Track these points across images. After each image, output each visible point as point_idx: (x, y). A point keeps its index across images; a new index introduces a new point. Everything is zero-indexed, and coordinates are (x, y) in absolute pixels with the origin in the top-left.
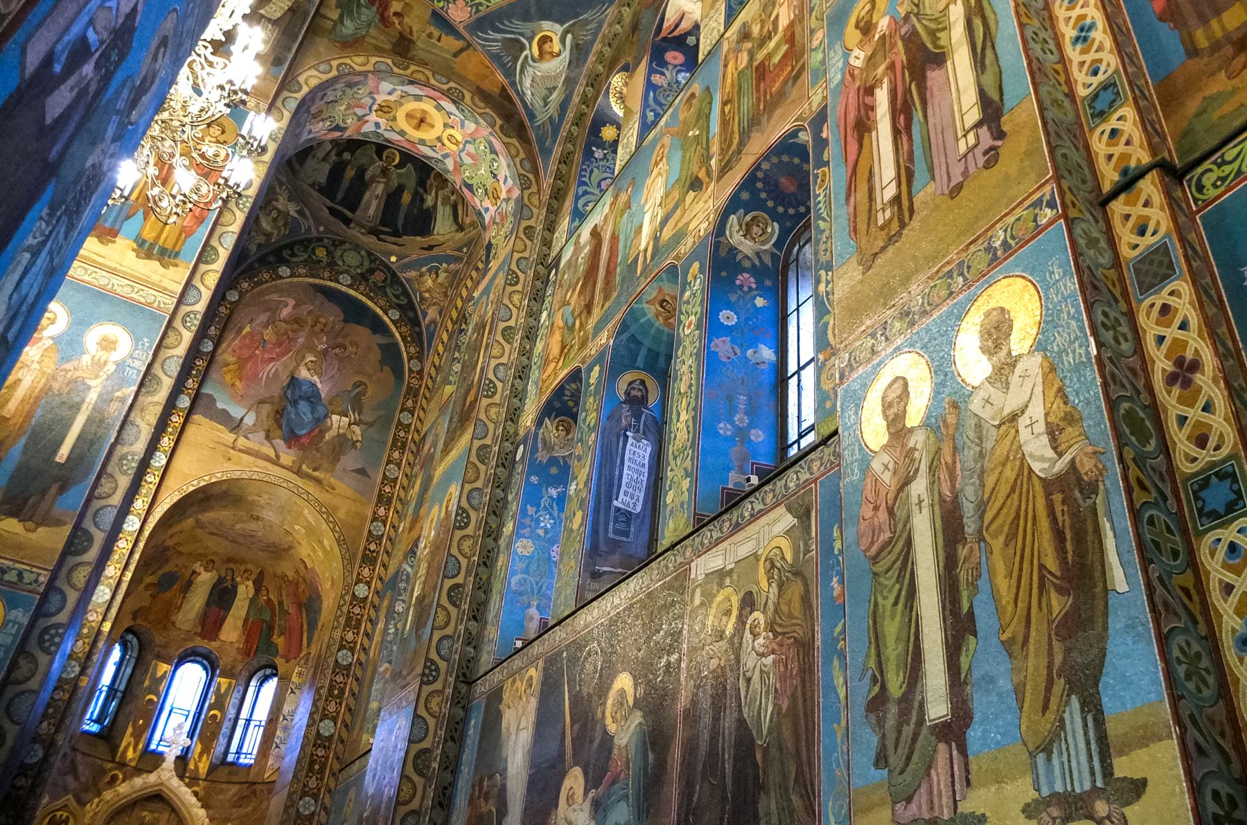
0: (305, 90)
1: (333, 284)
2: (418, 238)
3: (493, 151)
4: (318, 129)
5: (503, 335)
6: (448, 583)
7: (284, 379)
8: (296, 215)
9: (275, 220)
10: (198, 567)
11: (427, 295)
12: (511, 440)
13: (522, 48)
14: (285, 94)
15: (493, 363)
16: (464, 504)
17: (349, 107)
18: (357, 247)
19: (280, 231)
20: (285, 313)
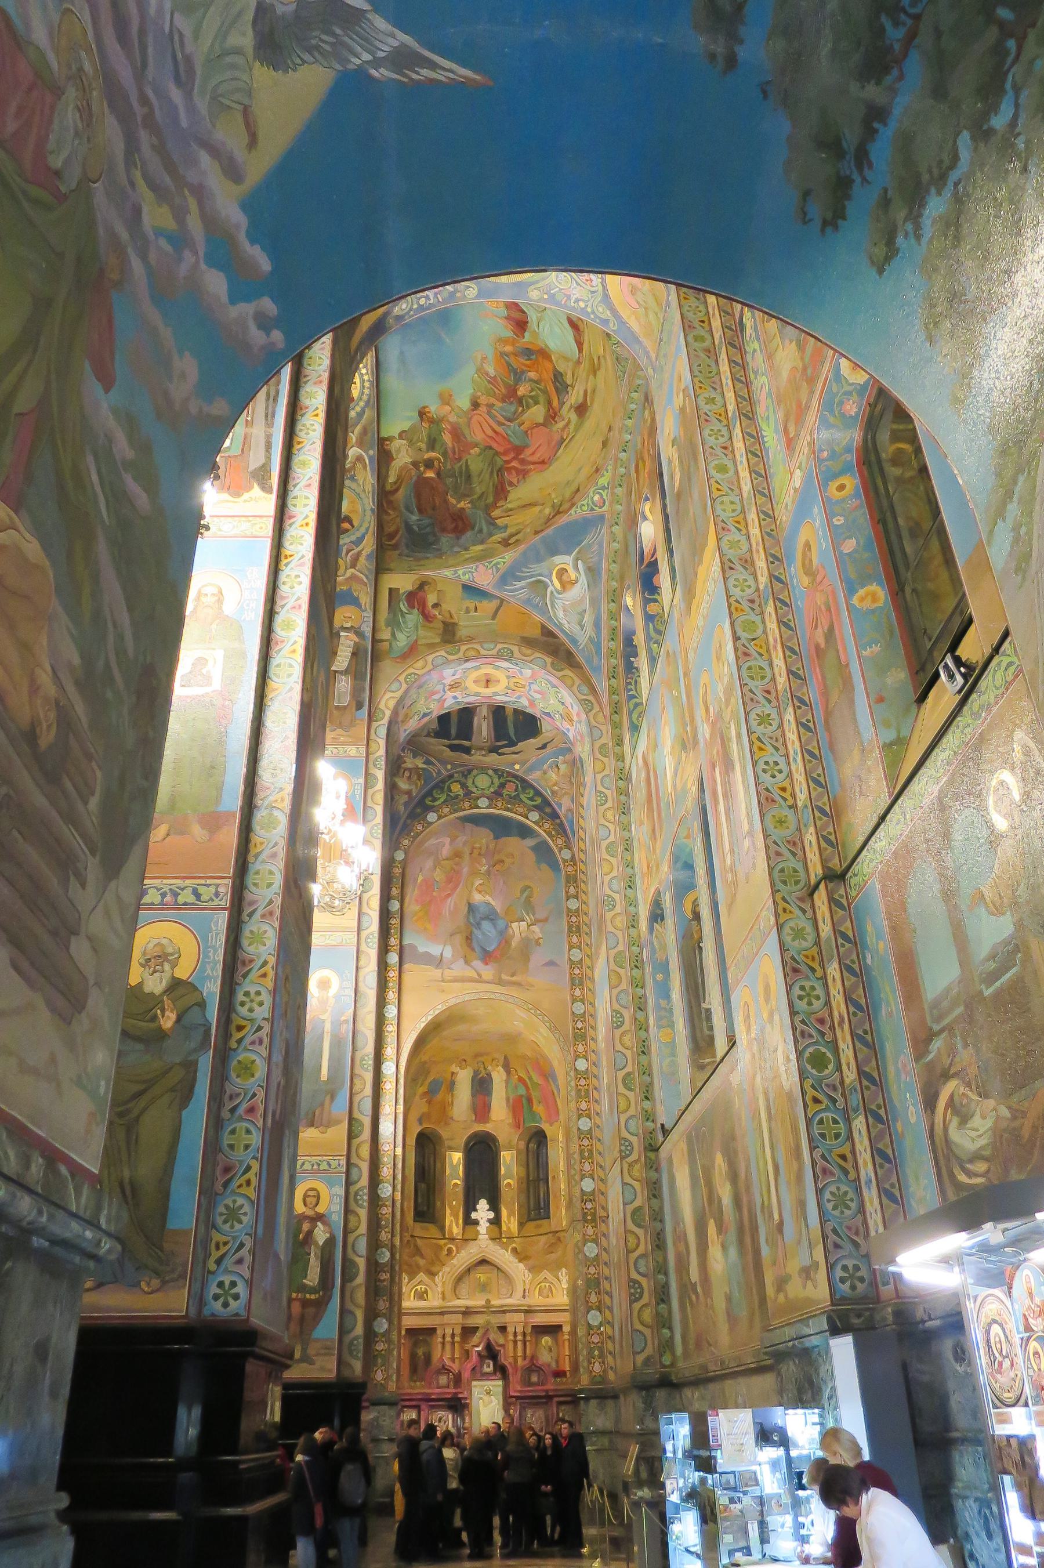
0: (388, 713)
2: (532, 740)
4: (413, 725)
5: (608, 852)
6: (621, 1074)
8: (424, 766)
9: (409, 778)
10: (454, 1068)
11: (556, 788)
13: (546, 586)
14: (374, 725)
15: (607, 879)
16: (616, 1007)
18: (483, 769)
19: (416, 785)
20: (446, 851)
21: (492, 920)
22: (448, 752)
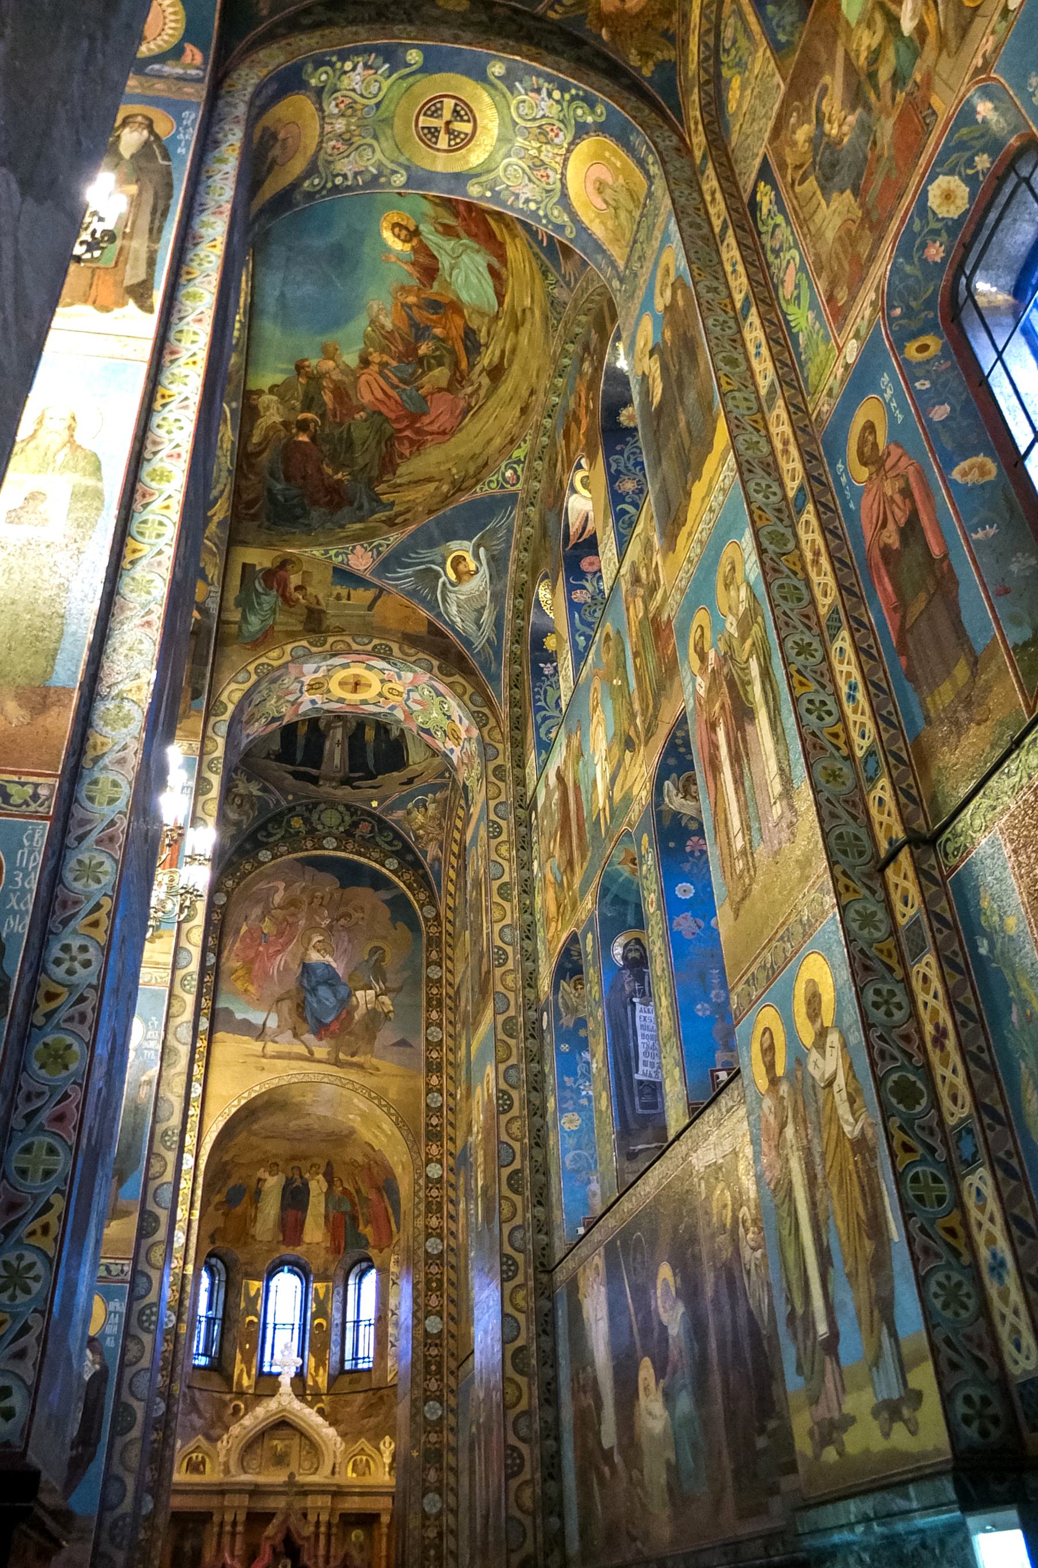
1: (319, 852)
3: (439, 694)
4: (256, 729)
5: (500, 894)
6: (506, 1172)
7: (296, 968)
8: (260, 794)
9: (240, 806)
10: (262, 1173)
12: (534, 1007)
13: (438, 576)
15: (497, 927)
16: (503, 1086)
17: (279, 698)
18: (332, 805)
20: (278, 898)
21: (331, 985)
22: (290, 780)
